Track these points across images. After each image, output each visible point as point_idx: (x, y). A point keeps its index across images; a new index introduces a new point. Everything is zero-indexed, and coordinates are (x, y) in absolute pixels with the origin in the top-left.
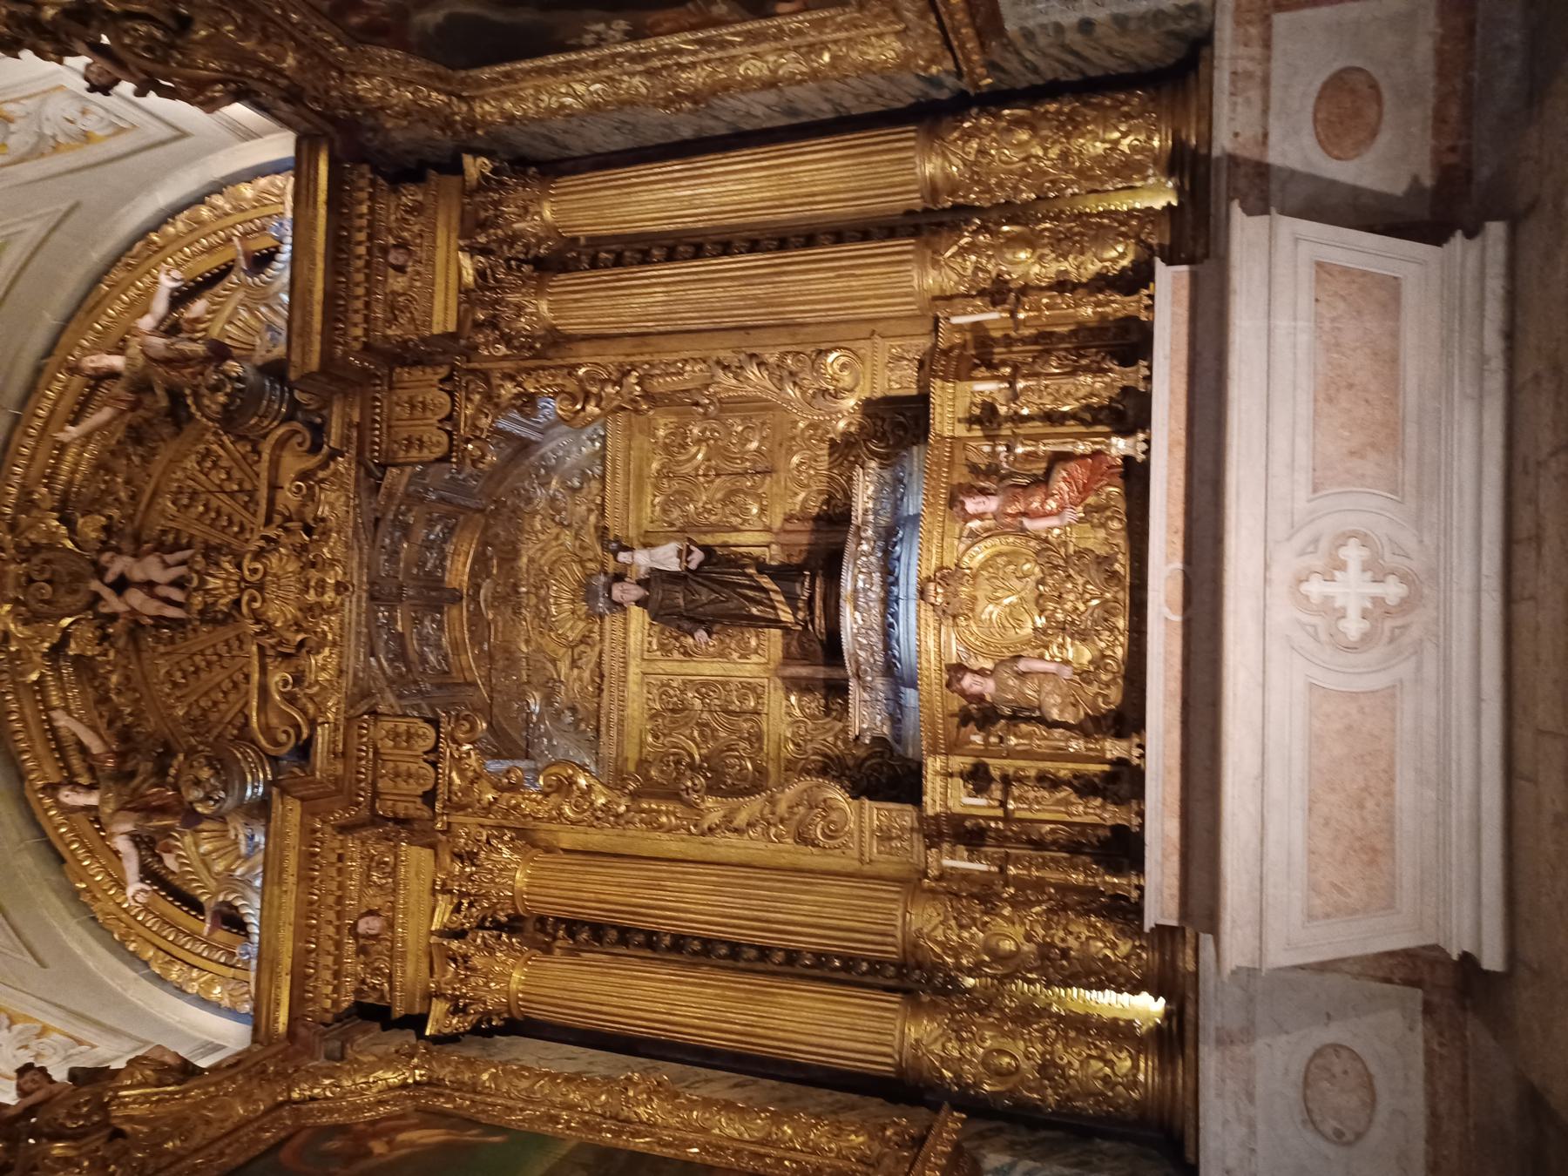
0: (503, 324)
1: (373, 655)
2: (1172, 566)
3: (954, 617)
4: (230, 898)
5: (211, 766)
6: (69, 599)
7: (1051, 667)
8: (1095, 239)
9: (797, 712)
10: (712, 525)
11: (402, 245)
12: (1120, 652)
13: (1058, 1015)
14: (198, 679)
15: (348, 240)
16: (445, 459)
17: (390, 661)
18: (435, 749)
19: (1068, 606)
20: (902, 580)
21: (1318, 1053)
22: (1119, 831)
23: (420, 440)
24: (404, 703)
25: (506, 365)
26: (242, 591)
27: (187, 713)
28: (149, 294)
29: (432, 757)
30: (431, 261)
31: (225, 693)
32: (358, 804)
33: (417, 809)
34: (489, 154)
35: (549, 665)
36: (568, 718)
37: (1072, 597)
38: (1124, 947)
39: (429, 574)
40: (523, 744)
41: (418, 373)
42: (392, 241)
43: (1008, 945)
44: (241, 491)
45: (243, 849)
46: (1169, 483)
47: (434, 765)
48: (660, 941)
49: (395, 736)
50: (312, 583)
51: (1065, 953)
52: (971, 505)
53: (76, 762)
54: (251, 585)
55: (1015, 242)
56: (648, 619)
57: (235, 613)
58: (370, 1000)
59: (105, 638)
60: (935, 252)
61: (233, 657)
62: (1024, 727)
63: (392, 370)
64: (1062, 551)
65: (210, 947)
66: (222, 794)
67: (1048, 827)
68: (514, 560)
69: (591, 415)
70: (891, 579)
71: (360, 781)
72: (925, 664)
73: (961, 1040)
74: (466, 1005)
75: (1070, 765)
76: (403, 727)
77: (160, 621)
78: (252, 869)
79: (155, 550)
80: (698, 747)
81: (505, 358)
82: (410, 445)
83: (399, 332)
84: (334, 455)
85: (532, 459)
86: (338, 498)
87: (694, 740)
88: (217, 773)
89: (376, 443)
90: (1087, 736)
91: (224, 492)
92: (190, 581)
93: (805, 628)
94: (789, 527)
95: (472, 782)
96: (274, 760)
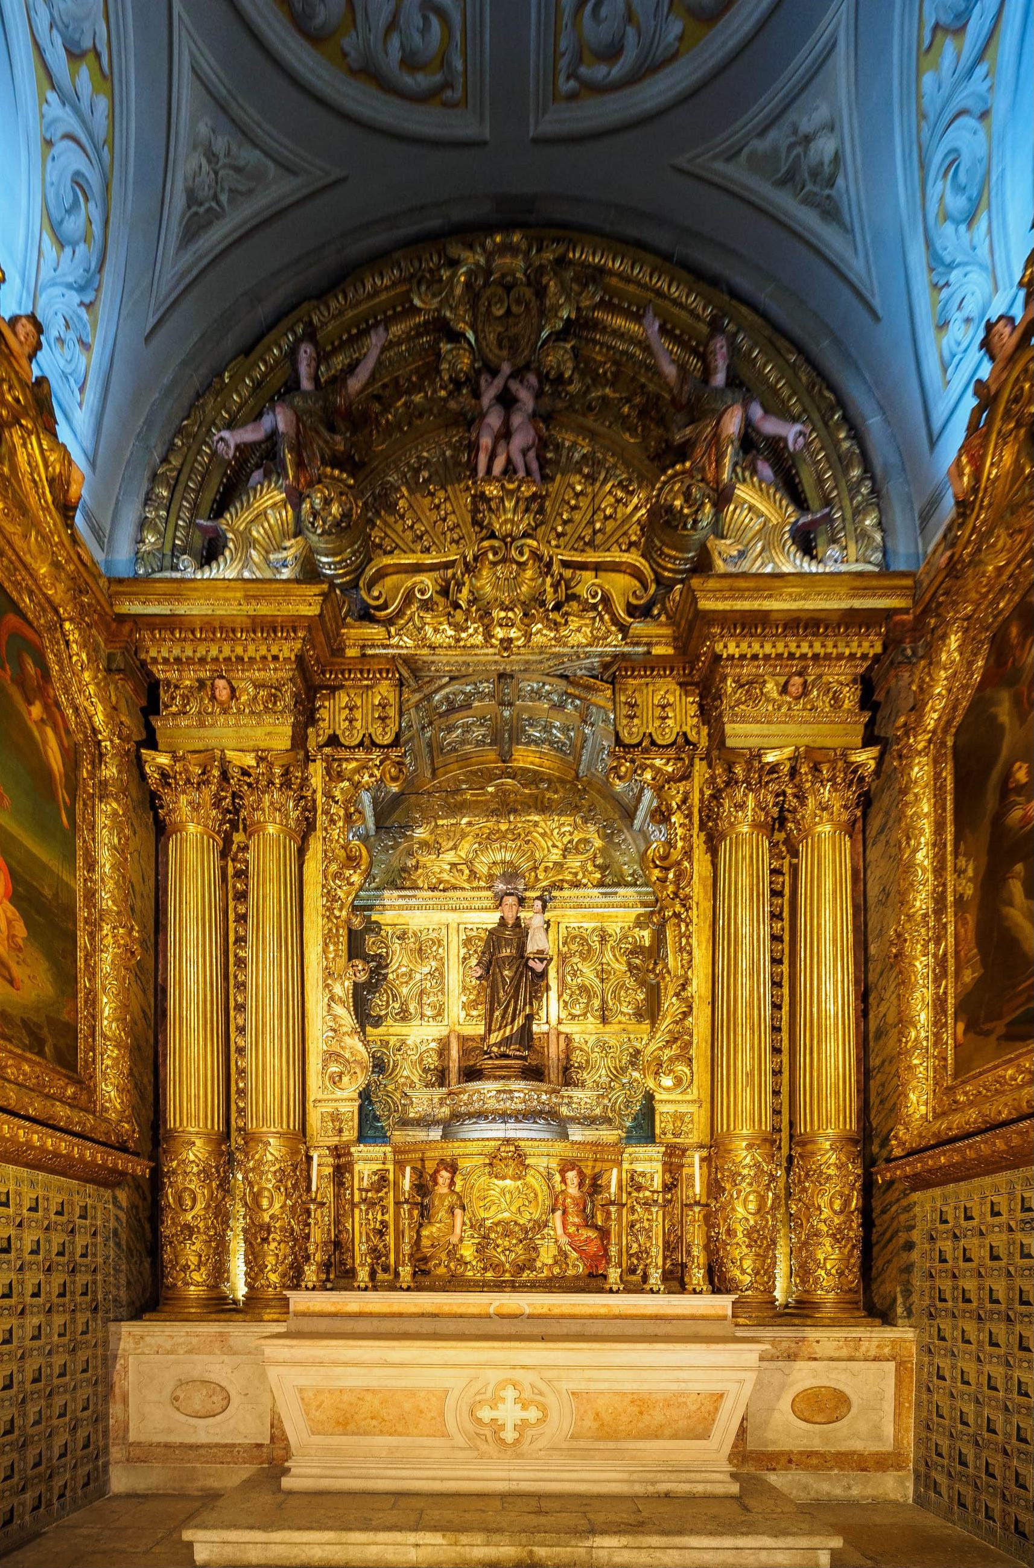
0: (729, 790)
6: (492, 337)
7: (458, 1230)
12: (470, 1273)
13: (225, 1235)
15: (816, 634)
16: (618, 741)
18: (374, 744)
21: (223, 1388)
22: (351, 1273)
23: (635, 716)
24: (412, 711)
26: (503, 540)
29: (367, 742)
30: (790, 718)
32: (323, 673)
34: (877, 772)
38: (274, 1278)
41: (693, 710)
42: (810, 679)
44: (595, 532)
50: (510, 614)
53: (340, 361)
58: (162, 693)
59: (458, 385)
61: (444, 533)
62: (416, 1212)
63: (697, 684)
66: (319, 531)
71: (343, 674)
72: (456, 1144)
73: (199, 1174)
74: (170, 784)
77: (473, 447)
79: (540, 438)
84: (624, 629)
90: (411, 1255)
92: (511, 481)
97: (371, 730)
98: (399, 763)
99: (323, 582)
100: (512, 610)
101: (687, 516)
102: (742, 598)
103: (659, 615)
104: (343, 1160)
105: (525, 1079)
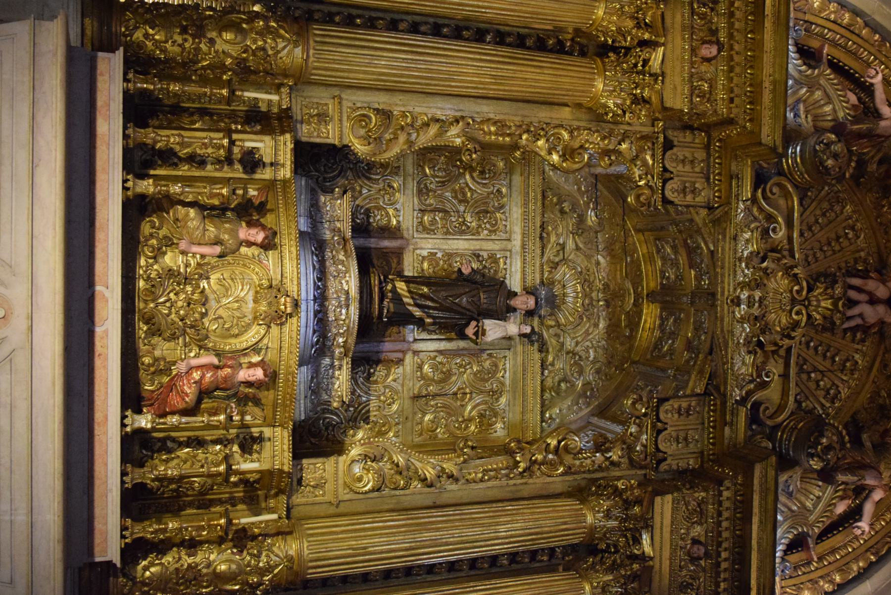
0: (621, 503)
1: (712, 252)
2: (103, 328)
3: (271, 287)
4: (809, 72)
5: (826, 168)
7: (195, 249)
8: (168, 581)
9: (391, 212)
10: (460, 356)
11: (694, 560)
12: (143, 262)
14: (836, 233)
15: (734, 562)
16: (662, 401)
17: (699, 247)
18: (665, 182)
19: (182, 296)
20: (311, 315)
23: (680, 414)
24: (689, 216)
25: (618, 474)
26: (807, 298)
27: (844, 207)
28: (877, 516)
29: (667, 175)
30: (673, 551)
31: (817, 222)
32: (720, 140)
33: (676, 136)
35: (581, 245)
36: (566, 206)
37: (180, 304)
38: (138, 35)
39: (671, 314)
40: (599, 186)
41: (682, 464)
43: (228, 36)
45: (801, 107)
46: (107, 393)
47: (665, 170)
48: (494, 38)
49: (693, 191)
50: (757, 305)
51: (184, 30)
52: (259, 374)
54: (801, 303)
55: (229, 577)
56: (507, 282)
57: (812, 282)
60: (291, 568)
61: (812, 249)
62: (216, 202)
63: (702, 466)
64: (187, 339)
65: (823, 36)
66: (818, 148)
67: (197, 126)
68: (609, 326)
69: (553, 438)
70: (320, 316)
71: (719, 157)
72: (293, 249)
75: (180, 173)
76: (689, 198)
77: (864, 275)
78: (795, 93)
79: (869, 327)
80: (467, 185)
81: (619, 478)
82: (688, 411)
83: (696, 495)
84: (743, 401)
85: (596, 403)
86: (739, 369)
87: (470, 189)
88: (822, 163)
89: (713, 411)
90: (167, 196)
91: (821, 372)
92: (844, 305)
93: (386, 277)
94: (400, 355)
95: (637, 156)
96: (781, 173)
97: (676, 179)
98: (649, 203)
99: (783, 148)
100: (760, 306)
101: (816, 449)
102: (761, 499)
103: (752, 430)
104: (276, 123)
105: (360, 318)
